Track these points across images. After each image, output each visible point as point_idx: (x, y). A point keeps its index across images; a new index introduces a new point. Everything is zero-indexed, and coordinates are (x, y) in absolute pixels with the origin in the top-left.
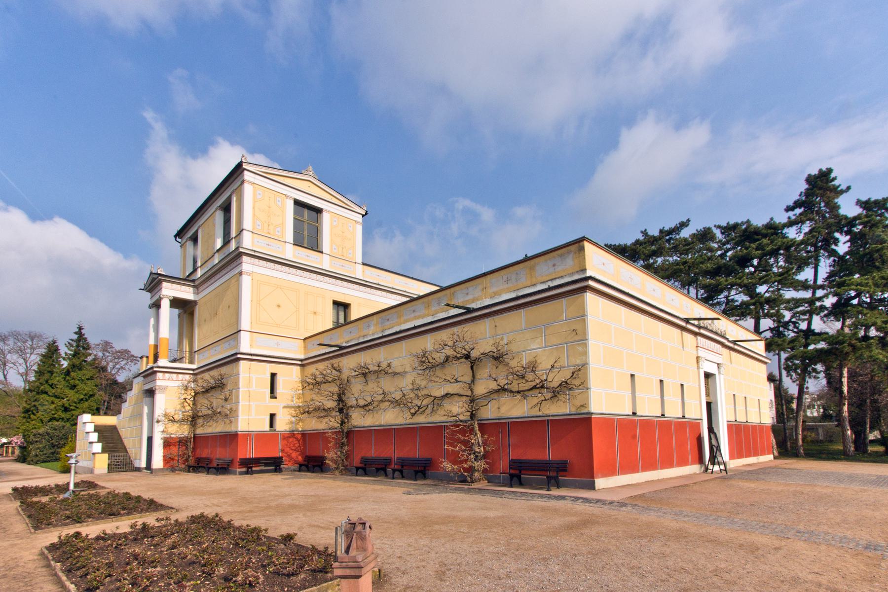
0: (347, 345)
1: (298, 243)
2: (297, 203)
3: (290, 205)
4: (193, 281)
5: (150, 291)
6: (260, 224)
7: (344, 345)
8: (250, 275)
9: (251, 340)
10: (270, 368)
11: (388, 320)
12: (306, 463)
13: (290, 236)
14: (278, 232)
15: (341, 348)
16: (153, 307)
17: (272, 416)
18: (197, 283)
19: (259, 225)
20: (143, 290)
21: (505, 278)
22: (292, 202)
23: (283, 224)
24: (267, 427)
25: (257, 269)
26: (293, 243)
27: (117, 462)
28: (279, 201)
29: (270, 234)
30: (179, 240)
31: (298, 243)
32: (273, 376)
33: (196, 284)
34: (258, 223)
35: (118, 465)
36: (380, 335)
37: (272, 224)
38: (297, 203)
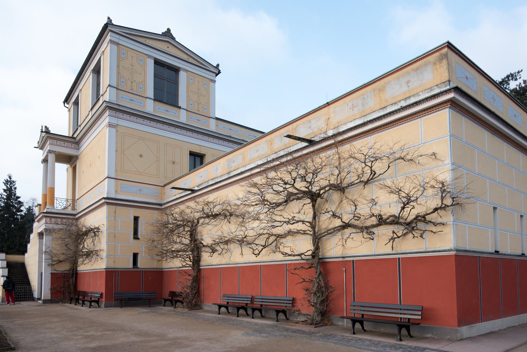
0: (199, 189)
1: (157, 99)
2: (157, 62)
5: (42, 148)
6: (124, 81)
7: (196, 188)
9: (116, 186)
10: (132, 212)
11: (234, 162)
12: (170, 298)
13: (150, 92)
14: (140, 88)
15: (193, 191)
16: (44, 162)
17: (135, 256)
18: (78, 138)
19: (123, 82)
21: (350, 105)
22: (152, 62)
23: (144, 82)
24: (131, 265)
26: (153, 98)
27: (20, 293)
28: (141, 60)
29: (133, 90)
31: (157, 99)
32: (136, 219)
34: (122, 80)
35: (21, 295)
36: (227, 177)
37: (135, 81)
38: (157, 62)
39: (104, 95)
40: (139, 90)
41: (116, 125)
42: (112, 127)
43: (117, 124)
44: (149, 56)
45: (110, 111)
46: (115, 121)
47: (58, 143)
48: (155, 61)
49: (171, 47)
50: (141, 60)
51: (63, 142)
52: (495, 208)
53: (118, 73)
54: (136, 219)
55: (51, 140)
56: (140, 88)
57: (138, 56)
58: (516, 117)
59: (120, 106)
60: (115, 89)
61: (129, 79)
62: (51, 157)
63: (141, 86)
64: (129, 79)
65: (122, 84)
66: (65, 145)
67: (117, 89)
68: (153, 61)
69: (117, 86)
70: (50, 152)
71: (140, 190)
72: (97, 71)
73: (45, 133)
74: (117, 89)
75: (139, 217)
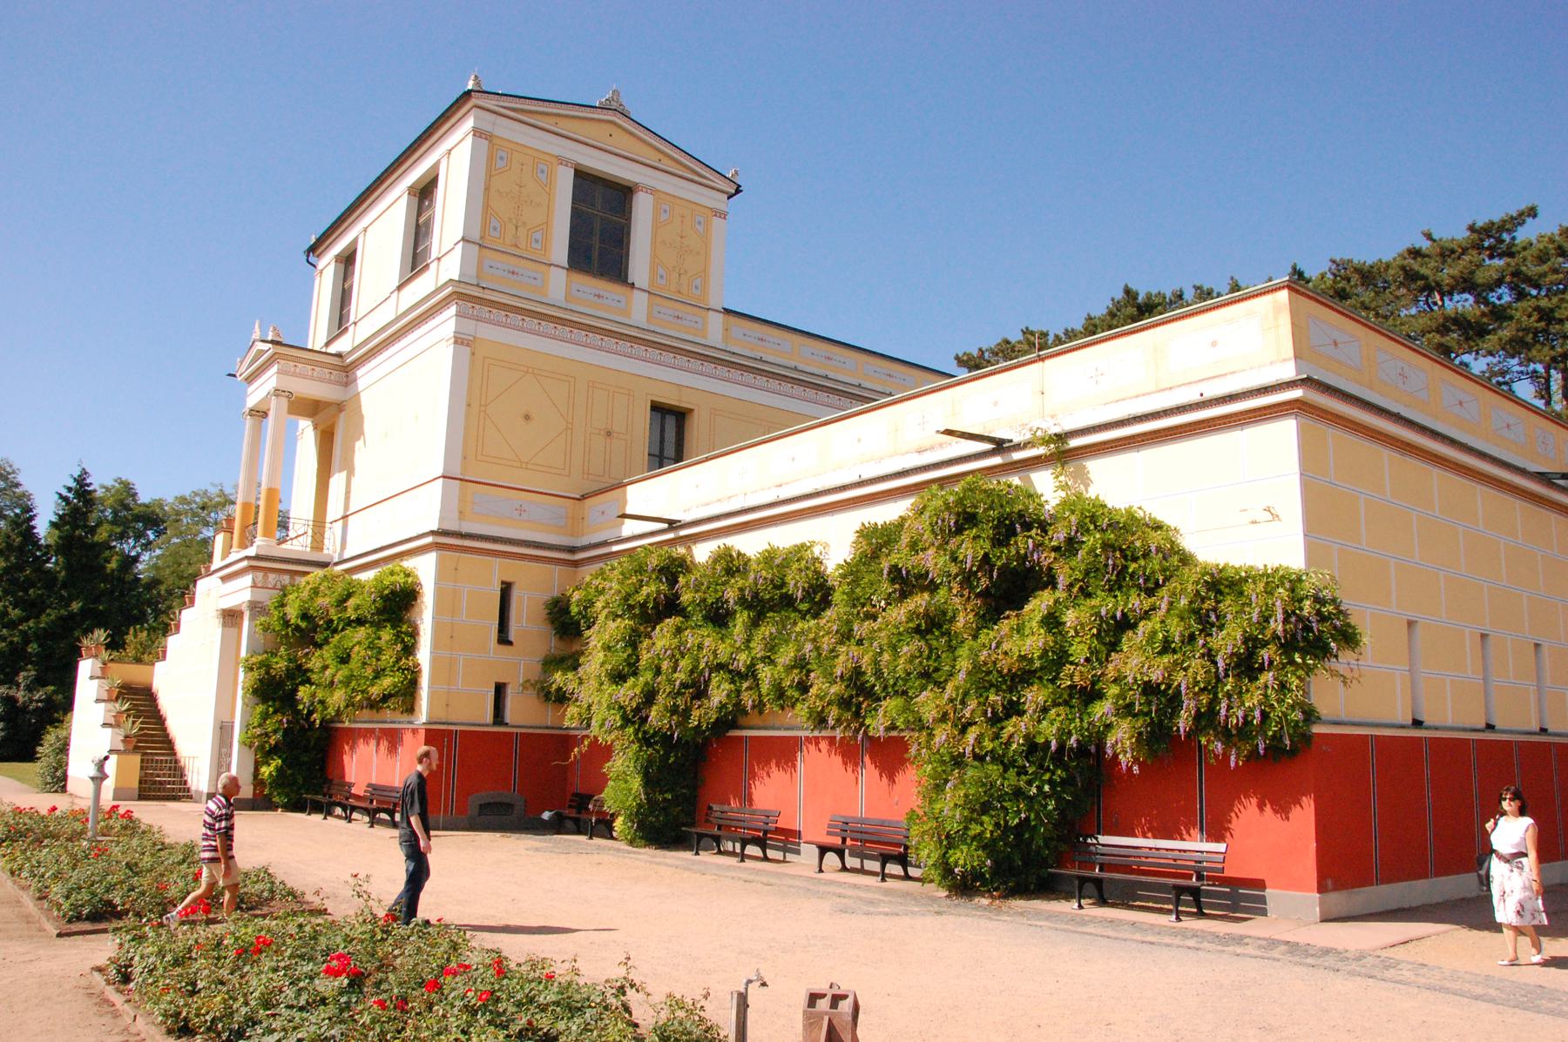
3: (565, 183)
4: (339, 355)
8: (468, 345)
14: (537, 241)
20: (234, 376)
25: (487, 332)
28: (542, 172)
30: (312, 259)
33: (345, 364)
34: (494, 223)
37: (524, 224)
39: (443, 259)
40: (534, 245)
41: (472, 338)
42: (462, 343)
43: (475, 338)
44: (562, 161)
45: (460, 302)
46: (470, 327)
47: (298, 371)
48: (575, 170)
49: (616, 132)
50: (542, 172)
51: (310, 367)
52: (1410, 624)
53: (487, 206)
54: (506, 590)
55: (282, 362)
56: (537, 241)
57: (536, 160)
58: (1465, 405)
59: (486, 291)
60: (477, 247)
61: (510, 219)
62: (276, 407)
63: (538, 236)
64: (510, 219)
65: (492, 233)
66: (315, 374)
67: (480, 245)
68: (573, 171)
69: (481, 238)
70: (277, 392)
71: (521, 510)
72: (425, 192)
73: (270, 345)
74: (480, 245)
75: (514, 583)
